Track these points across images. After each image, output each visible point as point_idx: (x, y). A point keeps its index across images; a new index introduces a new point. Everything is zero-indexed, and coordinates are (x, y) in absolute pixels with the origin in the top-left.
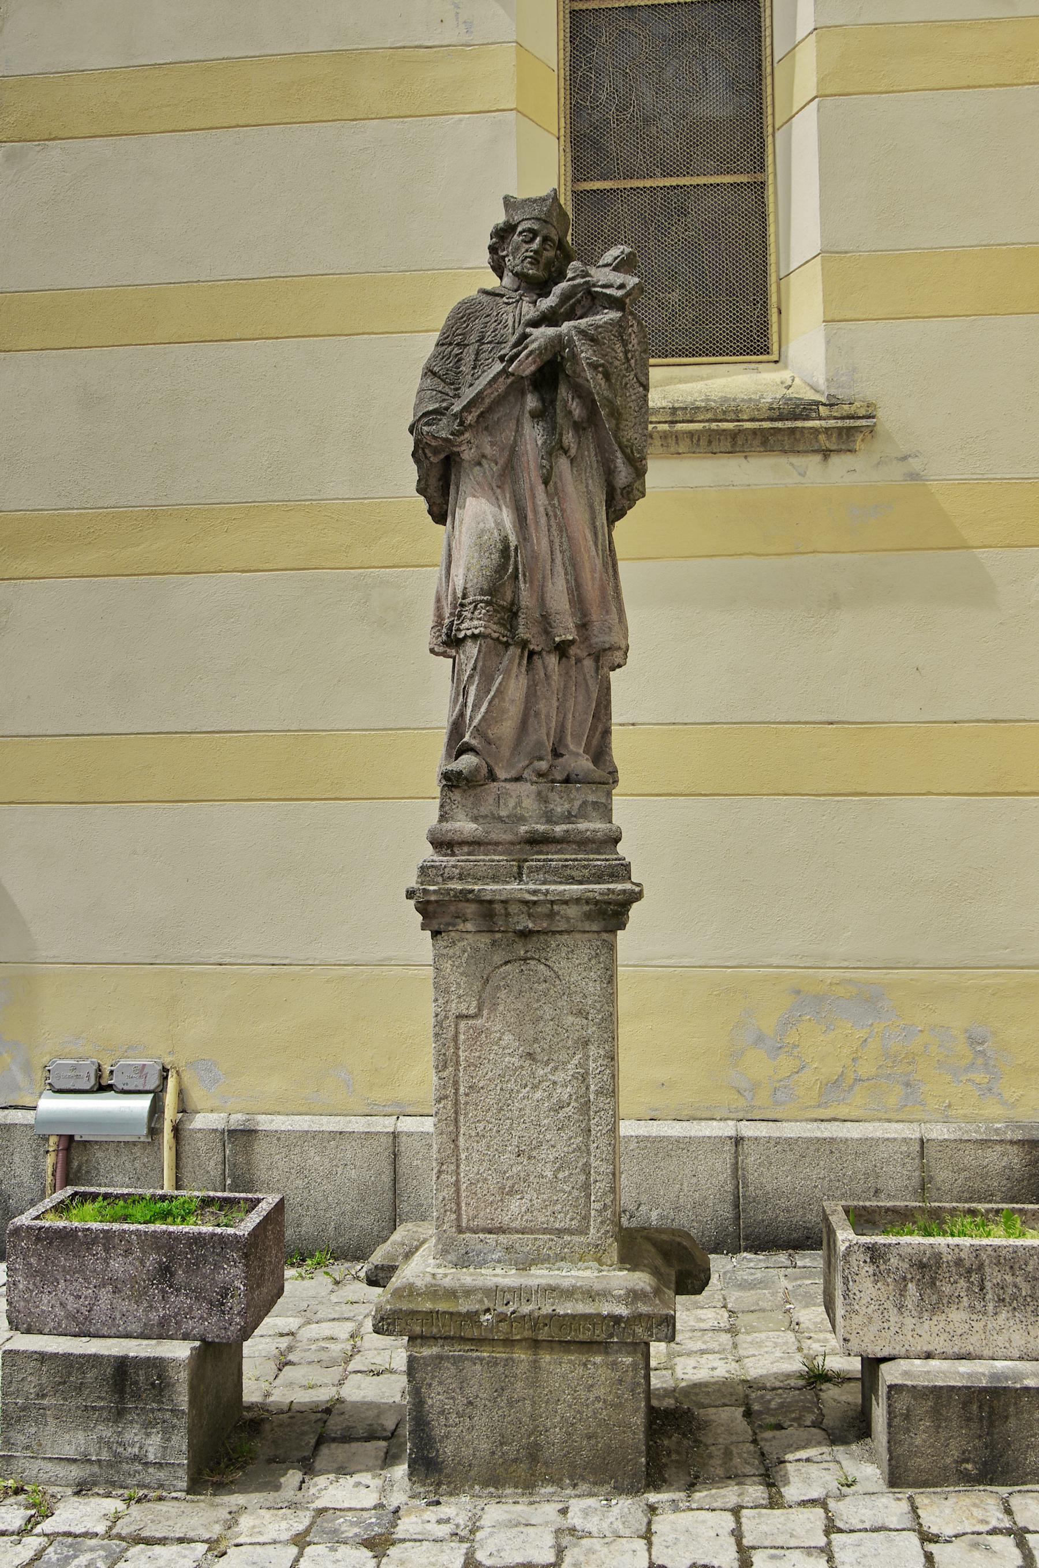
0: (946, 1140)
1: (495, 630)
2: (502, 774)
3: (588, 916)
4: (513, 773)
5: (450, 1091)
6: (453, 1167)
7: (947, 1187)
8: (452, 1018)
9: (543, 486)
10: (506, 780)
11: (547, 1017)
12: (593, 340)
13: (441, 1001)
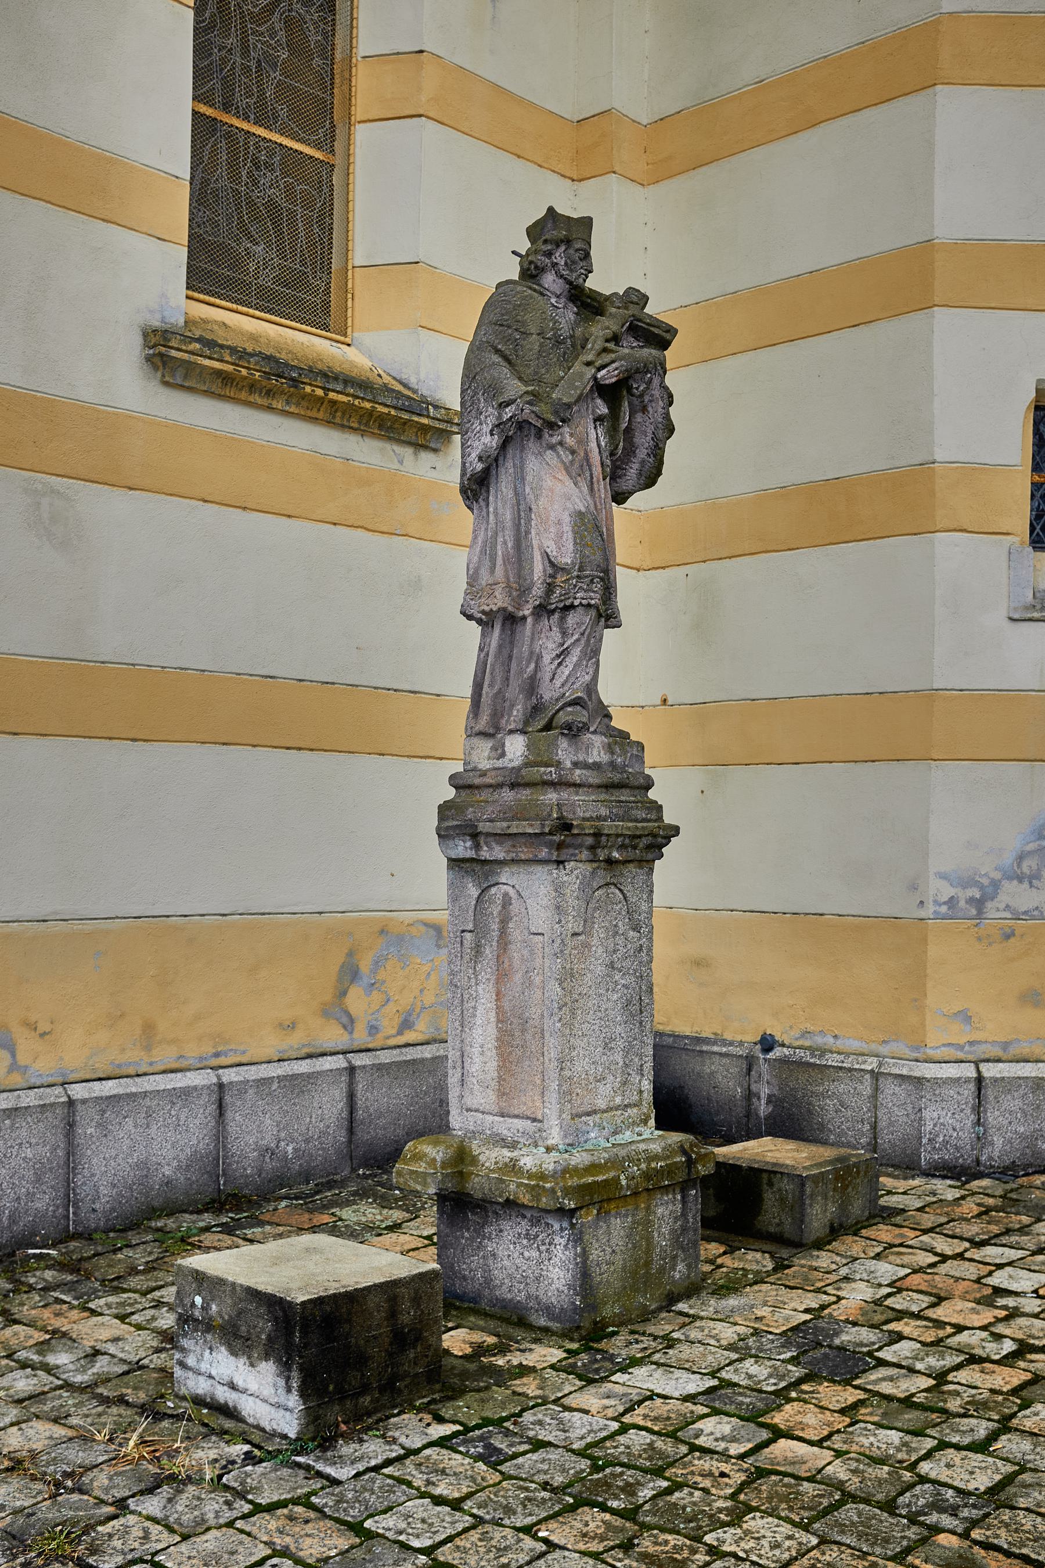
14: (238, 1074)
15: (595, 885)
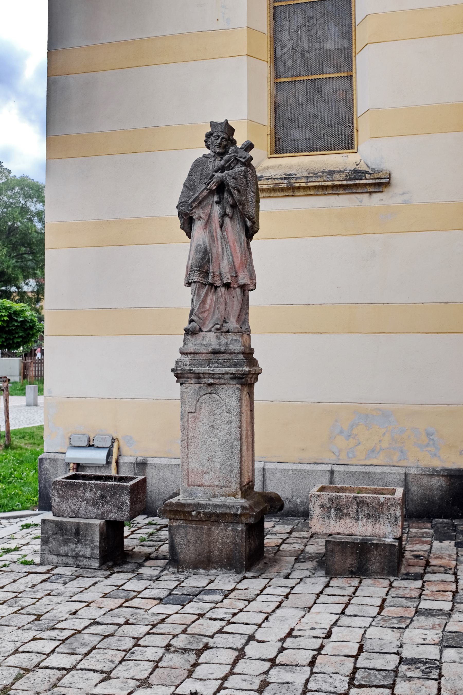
0: (415, 474)
1: (201, 280)
2: (205, 330)
3: (232, 378)
4: (208, 329)
5: (186, 438)
6: (187, 464)
7: (416, 493)
8: (186, 413)
9: (220, 228)
10: (206, 332)
11: (218, 413)
12: (234, 178)
13: (183, 407)
14: (274, 465)
15: (202, 393)
